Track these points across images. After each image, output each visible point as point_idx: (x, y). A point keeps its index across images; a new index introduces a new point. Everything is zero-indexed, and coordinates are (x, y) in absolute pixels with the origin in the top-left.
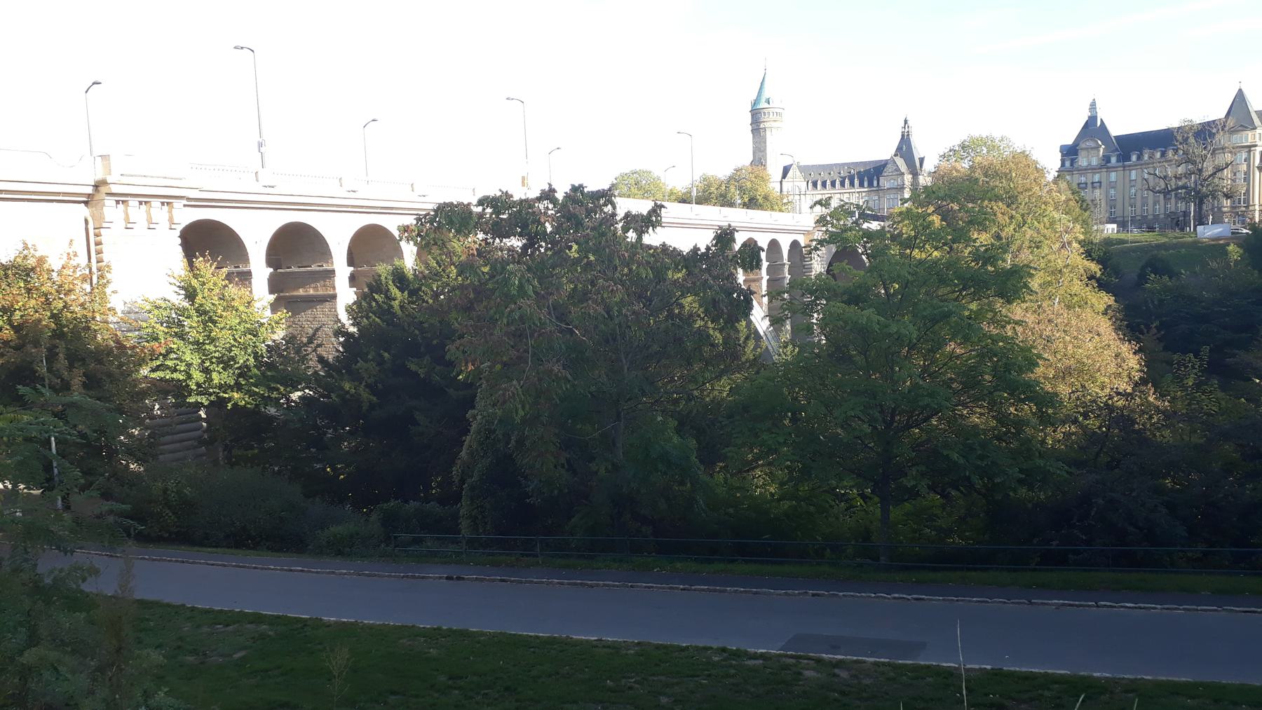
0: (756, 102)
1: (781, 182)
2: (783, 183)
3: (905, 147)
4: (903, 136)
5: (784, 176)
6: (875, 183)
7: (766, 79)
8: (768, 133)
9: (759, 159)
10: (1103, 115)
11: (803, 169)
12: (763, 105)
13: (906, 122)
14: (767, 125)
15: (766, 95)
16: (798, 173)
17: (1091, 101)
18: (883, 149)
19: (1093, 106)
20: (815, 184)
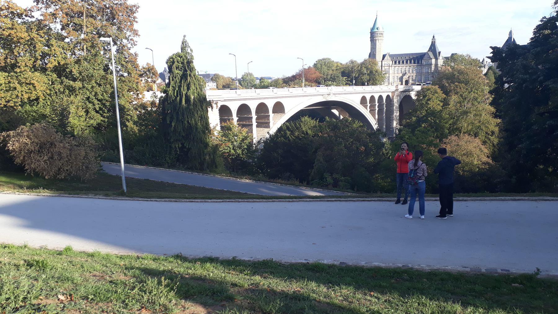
0: (372, 29)
1: (382, 61)
2: (383, 62)
3: (433, 48)
4: (432, 43)
5: (383, 59)
6: (420, 62)
7: (377, 20)
8: (377, 41)
9: (372, 55)
10: (514, 36)
11: (392, 56)
12: (376, 30)
13: (434, 37)
14: (377, 38)
15: (377, 26)
16: (389, 58)
17: (510, 31)
18: (424, 48)
19: (511, 33)
20: (395, 63)
